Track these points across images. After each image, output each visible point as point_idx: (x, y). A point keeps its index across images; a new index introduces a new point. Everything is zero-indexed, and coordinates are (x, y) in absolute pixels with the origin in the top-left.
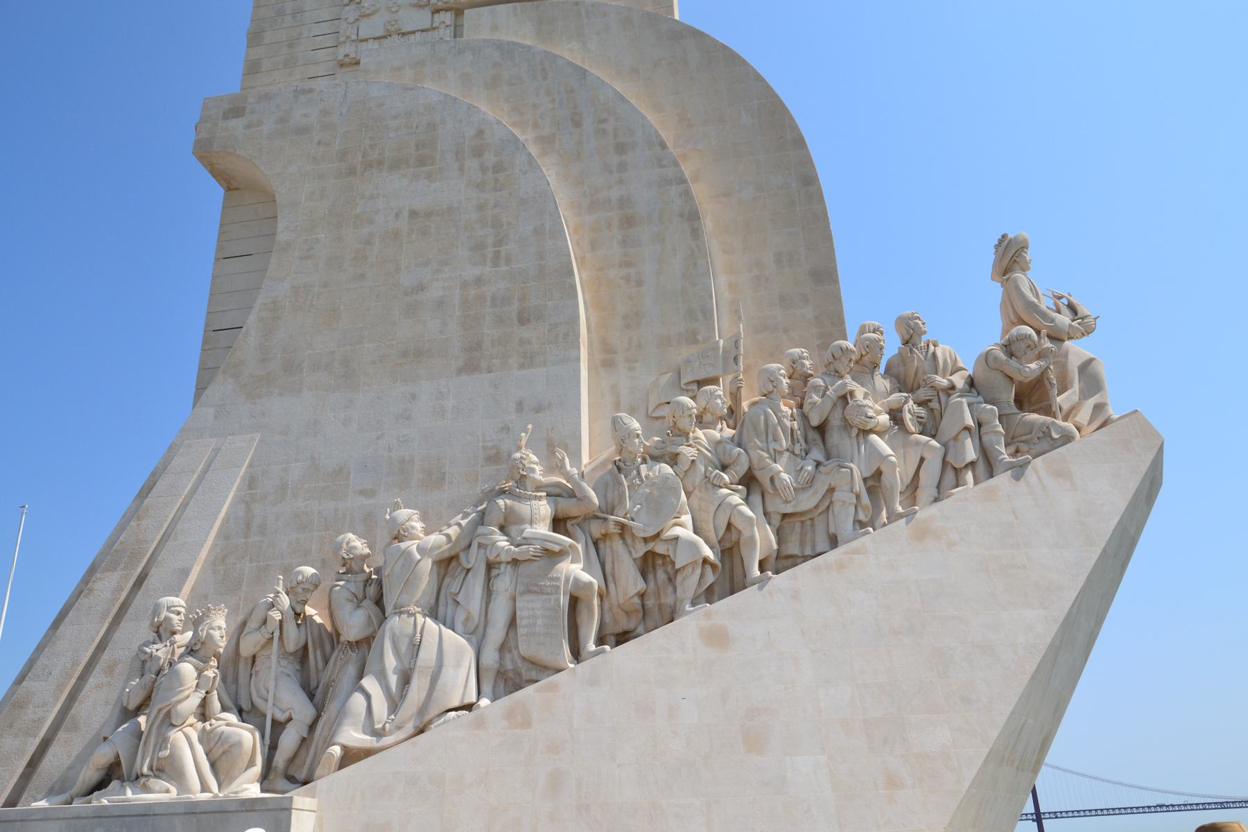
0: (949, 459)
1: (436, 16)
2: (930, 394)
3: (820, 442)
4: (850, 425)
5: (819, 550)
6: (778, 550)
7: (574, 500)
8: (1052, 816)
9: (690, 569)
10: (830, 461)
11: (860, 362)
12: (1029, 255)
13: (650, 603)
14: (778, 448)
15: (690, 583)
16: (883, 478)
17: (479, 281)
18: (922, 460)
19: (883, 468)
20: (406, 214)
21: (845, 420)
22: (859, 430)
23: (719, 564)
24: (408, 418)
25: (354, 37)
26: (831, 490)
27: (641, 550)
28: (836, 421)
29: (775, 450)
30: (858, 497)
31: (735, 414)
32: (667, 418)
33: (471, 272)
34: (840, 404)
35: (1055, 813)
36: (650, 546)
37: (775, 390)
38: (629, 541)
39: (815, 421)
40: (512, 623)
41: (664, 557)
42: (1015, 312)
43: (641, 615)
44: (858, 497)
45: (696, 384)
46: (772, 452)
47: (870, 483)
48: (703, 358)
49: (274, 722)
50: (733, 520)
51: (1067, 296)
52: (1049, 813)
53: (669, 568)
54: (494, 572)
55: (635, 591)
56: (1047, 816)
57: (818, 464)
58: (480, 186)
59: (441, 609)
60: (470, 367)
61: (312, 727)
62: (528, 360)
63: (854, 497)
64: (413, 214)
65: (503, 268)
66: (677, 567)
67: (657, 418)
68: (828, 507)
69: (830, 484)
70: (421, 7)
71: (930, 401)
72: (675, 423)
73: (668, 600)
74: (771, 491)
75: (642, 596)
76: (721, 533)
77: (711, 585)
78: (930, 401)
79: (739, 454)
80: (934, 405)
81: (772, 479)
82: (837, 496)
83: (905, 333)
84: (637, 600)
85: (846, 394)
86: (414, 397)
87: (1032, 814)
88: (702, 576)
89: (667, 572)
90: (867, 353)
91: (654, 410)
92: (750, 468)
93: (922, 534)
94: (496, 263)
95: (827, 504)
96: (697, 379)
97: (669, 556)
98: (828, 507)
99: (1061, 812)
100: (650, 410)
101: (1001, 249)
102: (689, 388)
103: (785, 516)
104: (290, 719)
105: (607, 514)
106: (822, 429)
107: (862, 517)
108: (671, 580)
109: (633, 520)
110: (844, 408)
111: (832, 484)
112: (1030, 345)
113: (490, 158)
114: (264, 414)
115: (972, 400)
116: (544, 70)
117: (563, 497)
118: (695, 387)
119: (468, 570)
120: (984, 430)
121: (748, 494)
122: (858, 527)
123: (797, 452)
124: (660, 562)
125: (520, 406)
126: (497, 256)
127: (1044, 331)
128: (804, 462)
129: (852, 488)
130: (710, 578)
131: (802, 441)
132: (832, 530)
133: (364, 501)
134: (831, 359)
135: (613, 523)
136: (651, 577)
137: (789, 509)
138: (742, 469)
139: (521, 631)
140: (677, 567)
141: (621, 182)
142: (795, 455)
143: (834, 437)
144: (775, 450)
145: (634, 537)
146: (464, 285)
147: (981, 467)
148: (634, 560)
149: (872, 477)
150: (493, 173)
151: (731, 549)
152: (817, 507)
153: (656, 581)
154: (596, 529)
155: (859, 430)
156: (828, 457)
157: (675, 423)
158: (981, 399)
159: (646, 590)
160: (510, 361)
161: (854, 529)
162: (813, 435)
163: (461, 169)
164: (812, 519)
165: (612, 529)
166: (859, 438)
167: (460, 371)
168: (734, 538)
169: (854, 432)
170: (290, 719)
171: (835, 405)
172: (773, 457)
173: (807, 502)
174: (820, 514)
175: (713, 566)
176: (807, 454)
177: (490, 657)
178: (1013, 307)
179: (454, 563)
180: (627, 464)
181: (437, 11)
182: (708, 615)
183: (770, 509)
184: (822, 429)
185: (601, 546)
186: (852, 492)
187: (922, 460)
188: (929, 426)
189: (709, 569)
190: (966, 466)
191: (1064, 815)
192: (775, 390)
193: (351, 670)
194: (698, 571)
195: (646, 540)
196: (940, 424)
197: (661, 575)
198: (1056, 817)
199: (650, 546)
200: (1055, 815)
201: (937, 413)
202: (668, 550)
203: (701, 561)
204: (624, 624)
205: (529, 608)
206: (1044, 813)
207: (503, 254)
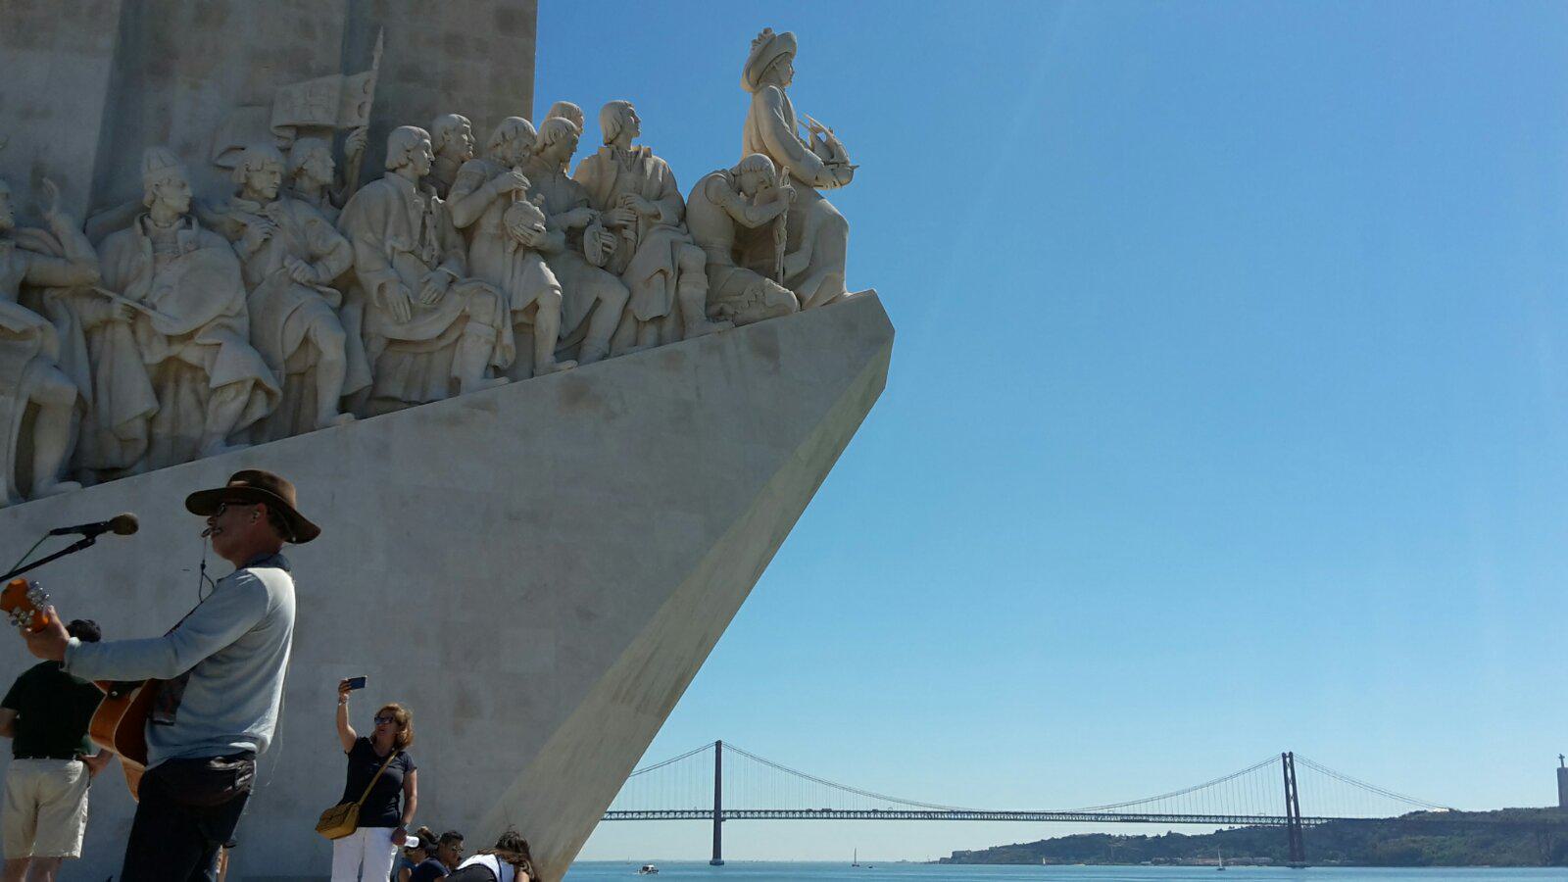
0: (632, 306)
2: (626, 218)
3: (462, 253)
4: (508, 235)
5: (430, 396)
6: (375, 386)
7: (61, 261)
9: (231, 393)
10: (470, 279)
11: (541, 154)
12: (796, 63)
13: (162, 430)
14: (399, 247)
15: (228, 409)
16: (539, 314)
18: (598, 301)
19: (541, 302)
21: (502, 226)
22: (519, 244)
23: (280, 393)
26: (465, 318)
27: (157, 354)
28: (490, 224)
29: (393, 248)
30: (499, 334)
31: (346, 187)
32: (236, 171)
34: (501, 202)
36: (177, 349)
37: (411, 164)
39: (460, 220)
41: (193, 368)
42: (760, 139)
43: (143, 445)
45: (294, 131)
46: (389, 251)
47: (521, 318)
48: (310, 96)
50: (311, 333)
51: (827, 130)
53: (201, 387)
55: (140, 411)
63: (494, 333)
66: (213, 385)
67: (225, 168)
68: (457, 340)
69: (463, 311)
71: (625, 227)
72: (247, 178)
74: (377, 305)
75: (151, 421)
77: (261, 421)
78: (625, 227)
79: (338, 245)
80: (629, 234)
81: (381, 288)
82: (470, 327)
83: (610, 128)
85: (511, 191)
88: (248, 406)
89: (195, 392)
90: (553, 143)
91: (222, 154)
92: (353, 267)
93: (576, 394)
95: (454, 335)
96: (297, 122)
97: (203, 369)
98: (457, 340)
101: (759, 47)
102: (282, 134)
103: (392, 342)
105: (114, 290)
106: (467, 233)
107: (498, 361)
108: (201, 404)
109: (154, 308)
110: (504, 211)
111: (467, 309)
112: (764, 181)
115: (677, 237)
117: (42, 253)
118: (290, 133)
120: (684, 277)
121: (344, 303)
122: (491, 372)
123: (425, 258)
124: (188, 376)
127: (785, 171)
128: (432, 274)
129: (493, 321)
130: (259, 410)
131: (436, 245)
132: (456, 372)
134: (499, 139)
135: (122, 306)
137: (398, 333)
138: (335, 266)
140: (213, 385)
142: (421, 260)
143: (481, 247)
144: (393, 248)
145: (152, 333)
147: (669, 326)
148: (146, 366)
149: (525, 310)
151: (302, 374)
152: (440, 337)
153: (176, 403)
154: (91, 311)
155: (519, 244)
156: (468, 274)
157: (247, 178)
158: (688, 238)
159: (158, 412)
161: (486, 376)
162: (452, 238)
164: (430, 353)
165: (117, 310)
166: (517, 255)
169: (513, 245)
171: (492, 203)
172: (390, 258)
173: (428, 329)
174: (442, 349)
175: (269, 394)
176: (440, 263)
178: (758, 129)
180: (160, 224)
183: (372, 329)
184: (467, 233)
185: (97, 338)
186: (492, 326)
187: (598, 301)
188: (617, 260)
189: (261, 396)
190: (653, 320)
192: (411, 164)
194: (243, 398)
195: (170, 339)
196: (632, 257)
197: (187, 397)
201: (631, 245)
202: (203, 359)
203: (249, 385)
204: (114, 457)
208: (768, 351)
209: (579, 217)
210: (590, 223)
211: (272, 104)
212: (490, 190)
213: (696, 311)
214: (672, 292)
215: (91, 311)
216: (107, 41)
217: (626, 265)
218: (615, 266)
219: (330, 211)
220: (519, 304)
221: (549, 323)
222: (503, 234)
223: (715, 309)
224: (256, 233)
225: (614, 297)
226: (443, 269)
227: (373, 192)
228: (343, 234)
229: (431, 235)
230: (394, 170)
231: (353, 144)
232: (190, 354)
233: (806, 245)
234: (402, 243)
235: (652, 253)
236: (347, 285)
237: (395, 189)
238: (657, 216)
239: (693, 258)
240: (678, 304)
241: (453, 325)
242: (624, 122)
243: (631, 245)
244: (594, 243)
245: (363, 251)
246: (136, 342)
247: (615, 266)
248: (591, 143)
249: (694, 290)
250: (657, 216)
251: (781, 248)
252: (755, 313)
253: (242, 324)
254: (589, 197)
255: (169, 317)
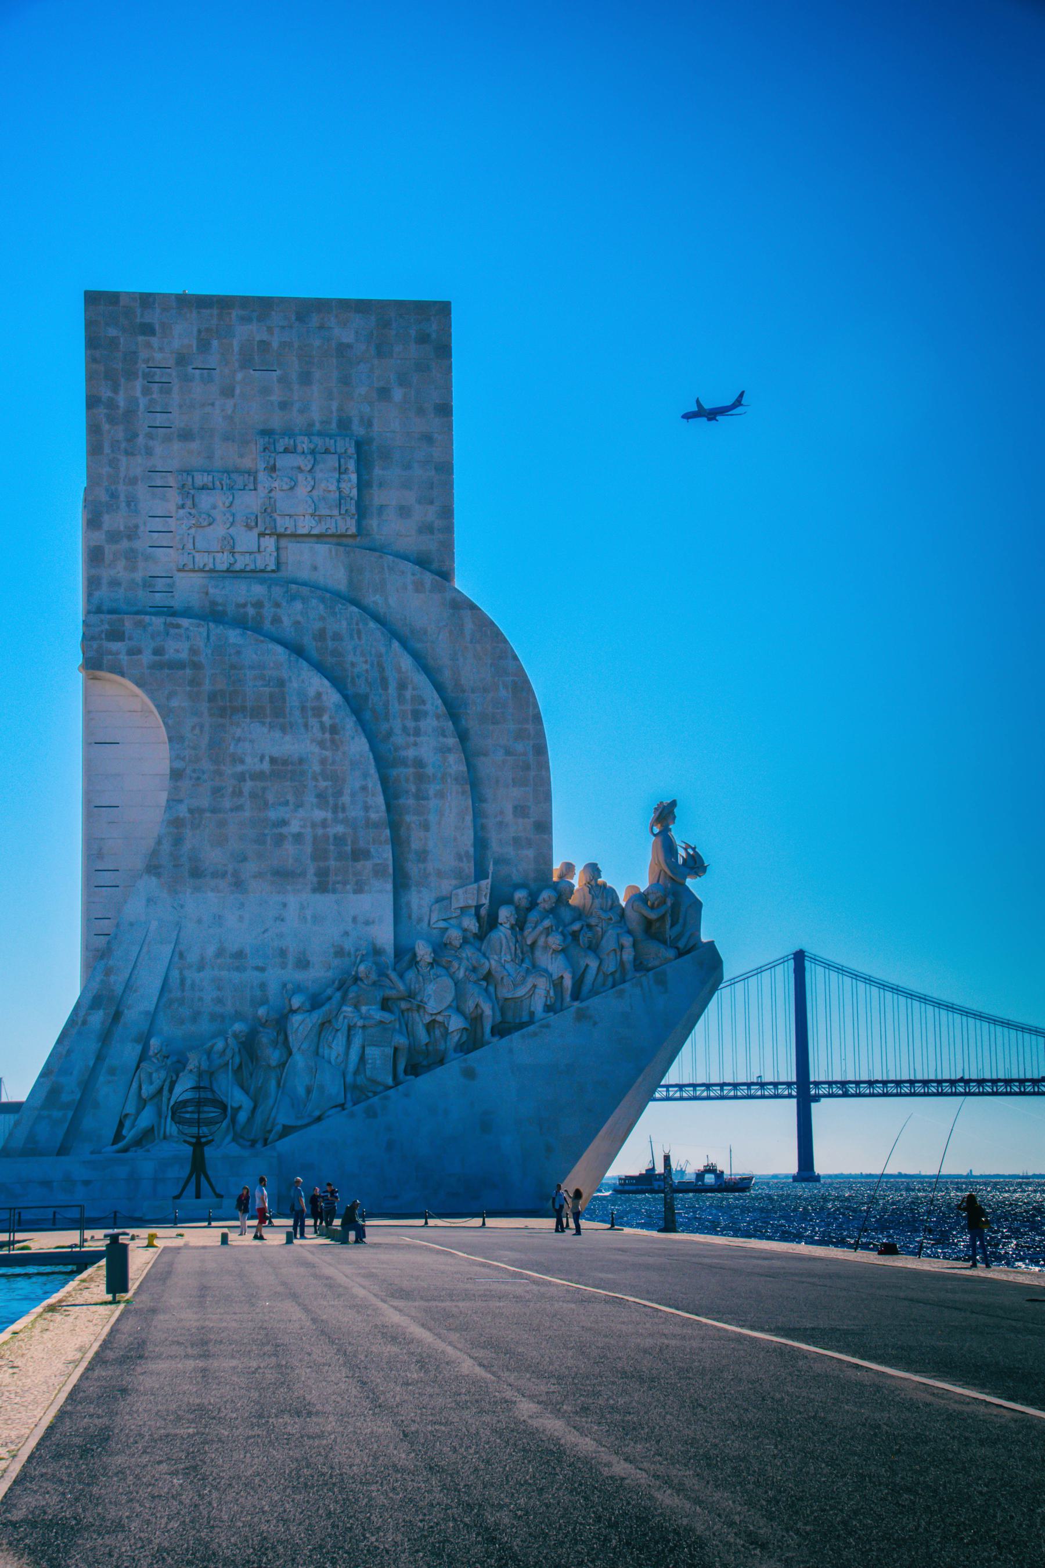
1: (262, 539)
8: (835, 1090)
17: (324, 824)
20: (267, 758)
21: (546, 942)
24: (282, 920)
25: (191, 546)
26: (535, 986)
27: (427, 1019)
28: (541, 941)
30: (548, 992)
33: (319, 815)
35: (843, 1084)
38: (422, 1014)
39: (529, 942)
40: (362, 1058)
44: (548, 992)
47: (557, 982)
49: (231, 1107)
52: (830, 1083)
54: (352, 1032)
56: (824, 1090)
57: (528, 970)
58: (321, 744)
59: (321, 1050)
60: (322, 887)
61: (254, 1110)
62: (359, 890)
64: (273, 760)
65: (341, 815)
66: (451, 1029)
70: (249, 528)
73: (442, 1047)
75: (427, 1045)
76: (471, 1010)
77: (464, 1042)
81: (502, 978)
84: (424, 1048)
86: (285, 905)
87: (789, 1084)
94: (335, 810)
99: (858, 1083)
100: (432, 923)
103: (506, 999)
104: (240, 1107)
106: (533, 945)
107: (548, 1003)
113: (326, 718)
114: (182, 906)
115: (619, 931)
116: (359, 632)
119: (337, 1030)
124: (437, 1026)
125: (355, 919)
126: (336, 806)
130: (464, 1039)
132: (532, 1009)
133: (256, 973)
136: (432, 1034)
139: (368, 1066)
141: (415, 744)
143: (538, 953)
145: (425, 1011)
146: (314, 825)
147: (617, 975)
150: (331, 734)
160: (348, 887)
162: (526, 948)
163: (306, 726)
164: (522, 1001)
167: (314, 891)
168: (479, 1011)
169: (551, 950)
170: (240, 1107)
171: (541, 933)
173: (521, 992)
177: (349, 1079)
179: (327, 1024)
181: (261, 535)
182: (465, 1060)
184: (533, 945)
185: (406, 1014)
187: (587, 966)
191: (864, 1089)
193: (273, 1083)
195: (432, 1014)
198: (846, 1095)
199: (434, 1017)
200: (844, 1089)
205: (372, 1052)
206: (817, 1084)
207: (340, 803)
208: (661, 981)
209: (576, 927)
210: (582, 929)
211: (451, 898)
212: (540, 928)
213: (629, 967)
214: (619, 958)
215: (403, 1005)
216: (389, 887)
217: (598, 945)
218: (594, 948)
219: (477, 944)
220: (555, 977)
221: (568, 983)
222: (546, 947)
223: (638, 962)
224: (456, 964)
225: (594, 964)
226: (524, 965)
227: (494, 935)
228: (484, 955)
229: (519, 951)
230: (501, 924)
231: (483, 912)
232: (439, 1018)
233: (681, 920)
234: (508, 958)
235: (609, 943)
236: (488, 977)
237: (502, 933)
238: (611, 919)
239: (627, 941)
240: (622, 963)
241: (529, 991)
242: (593, 870)
243: (600, 933)
244: (583, 939)
245: (493, 963)
246: (420, 1015)
247: (594, 948)
248: (576, 881)
249: (628, 955)
250: (611, 919)
251: (668, 927)
252: (657, 963)
253: (454, 1004)
254: (579, 914)
255: (432, 1006)
